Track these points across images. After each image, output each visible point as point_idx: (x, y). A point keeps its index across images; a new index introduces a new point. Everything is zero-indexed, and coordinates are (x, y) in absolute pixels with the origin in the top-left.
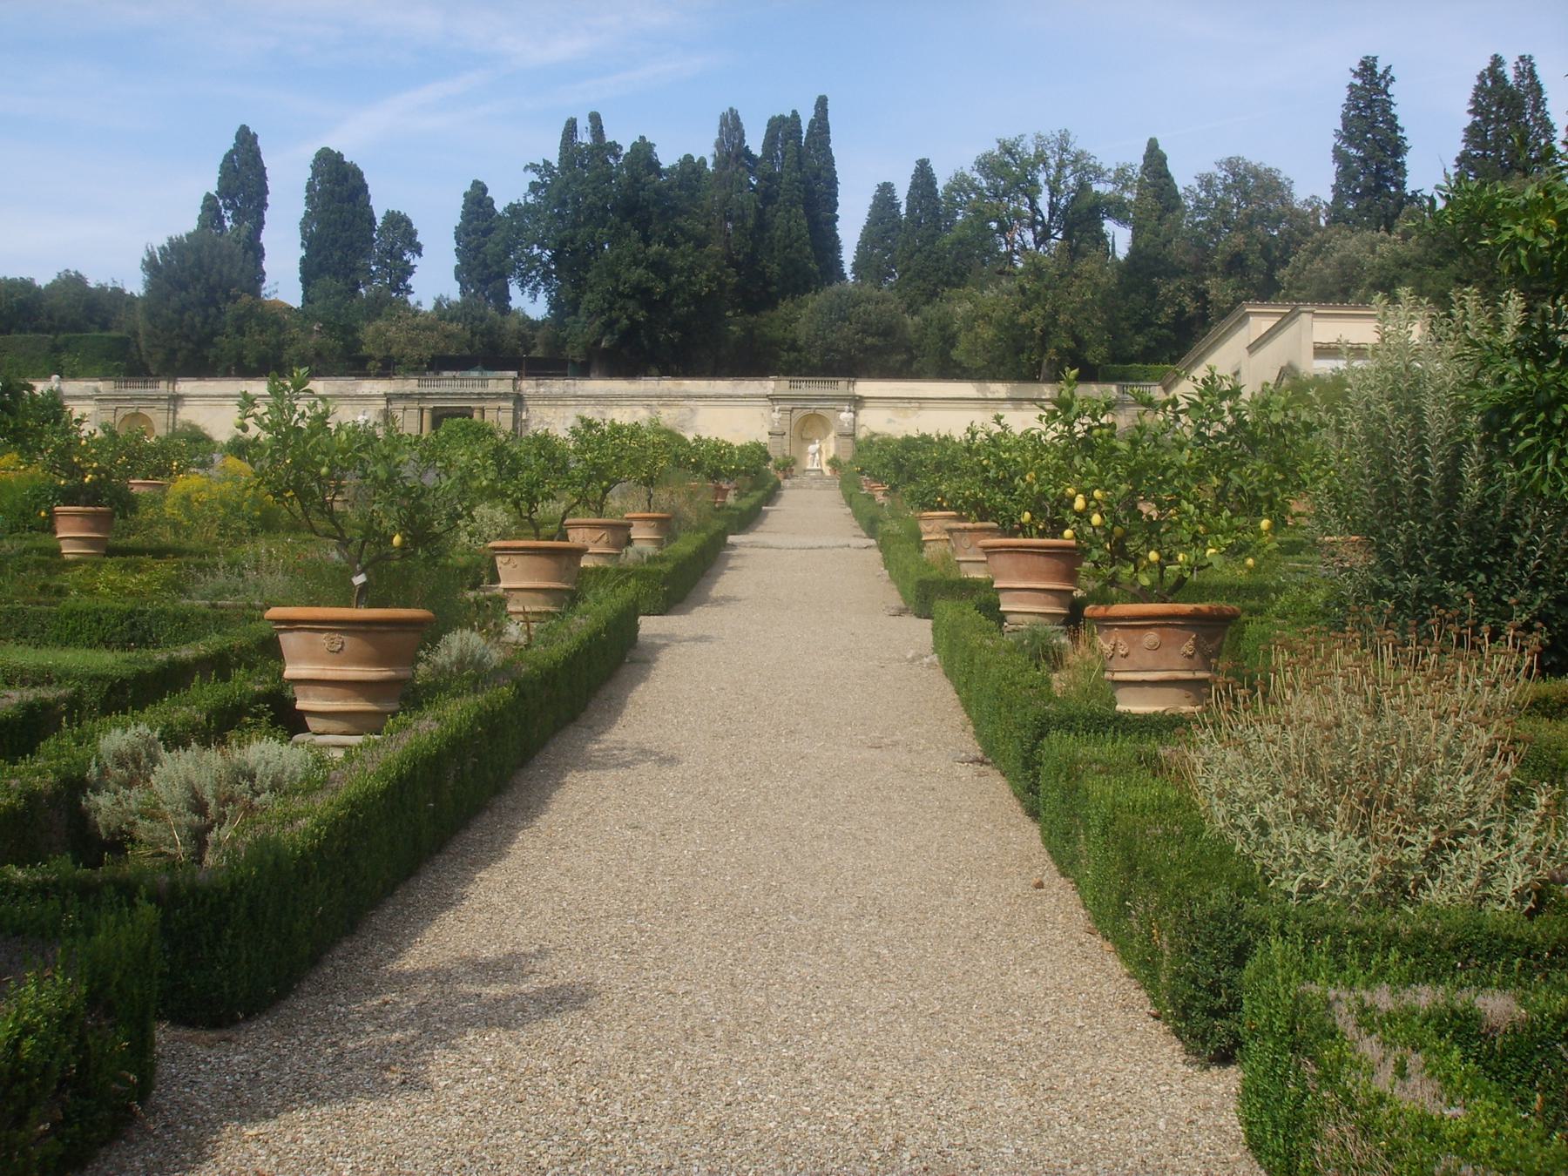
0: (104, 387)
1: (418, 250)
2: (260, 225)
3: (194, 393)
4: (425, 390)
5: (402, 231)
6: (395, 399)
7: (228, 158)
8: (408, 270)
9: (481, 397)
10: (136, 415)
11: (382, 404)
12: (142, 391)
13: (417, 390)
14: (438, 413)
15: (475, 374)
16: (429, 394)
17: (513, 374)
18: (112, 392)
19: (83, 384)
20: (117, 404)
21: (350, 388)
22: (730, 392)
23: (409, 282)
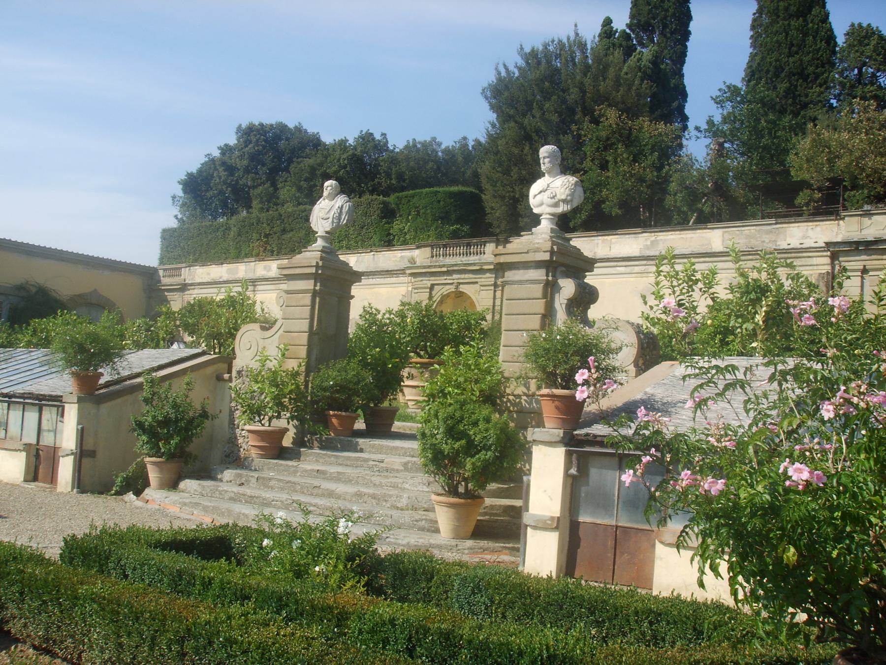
0: (421, 255)
6: (847, 253)
12: (465, 259)
18: (427, 262)
21: (766, 238)
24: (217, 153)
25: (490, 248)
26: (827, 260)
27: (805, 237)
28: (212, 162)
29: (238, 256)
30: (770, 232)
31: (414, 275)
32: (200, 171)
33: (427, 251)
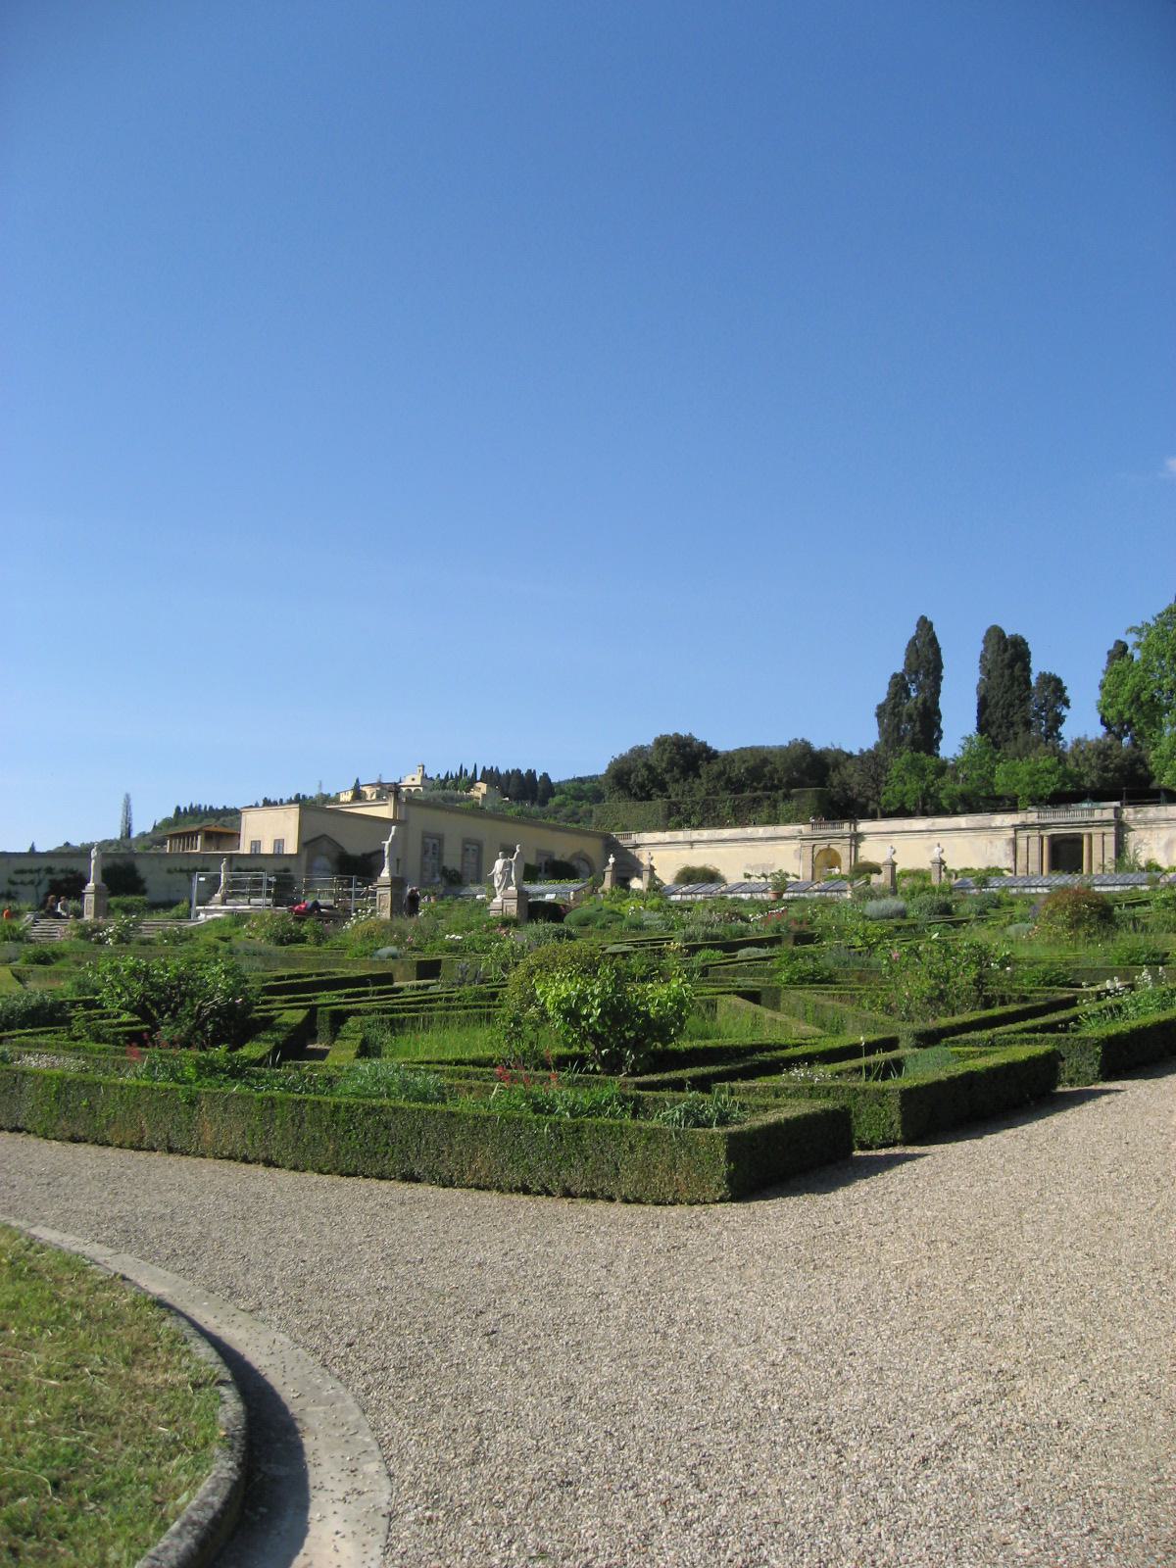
0: (805, 829)
1: (1066, 703)
2: (938, 692)
3: (869, 831)
5: (1055, 688)
6: (1021, 829)
7: (912, 643)
8: (1059, 720)
9: (1088, 824)
10: (829, 849)
11: (1010, 833)
13: (1037, 821)
14: (1056, 839)
17: (1116, 804)
18: (811, 833)
19: (791, 827)
20: (814, 842)
23: (1060, 730)
25: (846, 826)
27: (1003, 821)
31: (802, 839)
33: (809, 827)
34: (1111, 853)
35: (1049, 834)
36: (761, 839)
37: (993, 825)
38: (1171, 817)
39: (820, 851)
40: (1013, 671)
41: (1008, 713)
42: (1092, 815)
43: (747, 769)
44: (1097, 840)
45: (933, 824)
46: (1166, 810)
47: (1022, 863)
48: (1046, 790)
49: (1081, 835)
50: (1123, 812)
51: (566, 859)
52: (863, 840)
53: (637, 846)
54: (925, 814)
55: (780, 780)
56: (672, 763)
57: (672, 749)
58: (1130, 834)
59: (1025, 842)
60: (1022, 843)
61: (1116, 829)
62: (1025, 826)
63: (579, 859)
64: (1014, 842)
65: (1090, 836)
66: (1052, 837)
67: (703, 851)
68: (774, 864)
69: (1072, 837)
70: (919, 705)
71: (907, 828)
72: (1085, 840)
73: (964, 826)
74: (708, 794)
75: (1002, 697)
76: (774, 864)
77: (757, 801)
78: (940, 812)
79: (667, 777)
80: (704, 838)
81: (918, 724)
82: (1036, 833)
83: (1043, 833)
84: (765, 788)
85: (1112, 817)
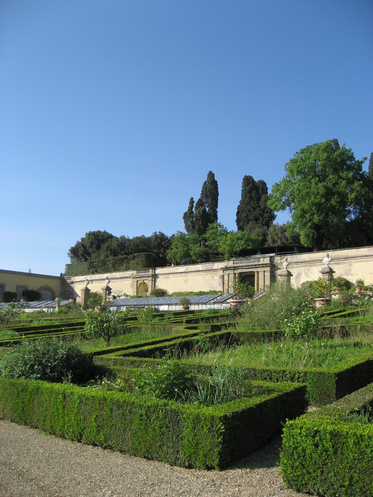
0: (134, 272)
4: (236, 265)
9: (256, 266)
13: (232, 265)
14: (243, 275)
15: (258, 256)
16: (238, 267)
19: (129, 272)
22: (367, 254)
24: (80, 241)
25: (151, 270)
26: (222, 272)
28: (78, 243)
29: (88, 274)
30: (211, 265)
31: (133, 278)
32: (75, 247)
33: (136, 271)
34: (268, 282)
35: (238, 272)
36: (117, 278)
37: (214, 268)
38: (298, 261)
39: (140, 284)
40: (251, 194)
41: (248, 215)
42: (259, 261)
43: (117, 245)
44: (261, 275)
45: (187, 269)
46: (296, 257)
47: (226, 287)
48: (238, 249)
49: (254, 272)
50: (274, 259)
51: (36, 289)
52: (158, 277)
53: (73, 283)
54: (185, 264)
55: (132, 249)
56: (92, 243)
57: (92, 237)
58: (278, 271)
59: (227, 277)
60: (226, 277)
61: (270, 269)
62: (226, 269)
63: (45, 289)
64: (223, 277)
65: (258, 272)
66: (240, 274)
67: (96, 284)
68: (122, 290)
69: (250, 274)
70: (201, 212)
71: (176, 271)
72: (256, 275)
73: (201, 269)
74: (105, 258)
75: (246, 207)
76: (122, 290)
77: (122, 260)
78: (194, 262)
79: (90, 250)
80: (97, 278)
81: (200, 221)
82: (232, 272)
83: (236, 272)
84: (125, 253)
85: (269, 262)
